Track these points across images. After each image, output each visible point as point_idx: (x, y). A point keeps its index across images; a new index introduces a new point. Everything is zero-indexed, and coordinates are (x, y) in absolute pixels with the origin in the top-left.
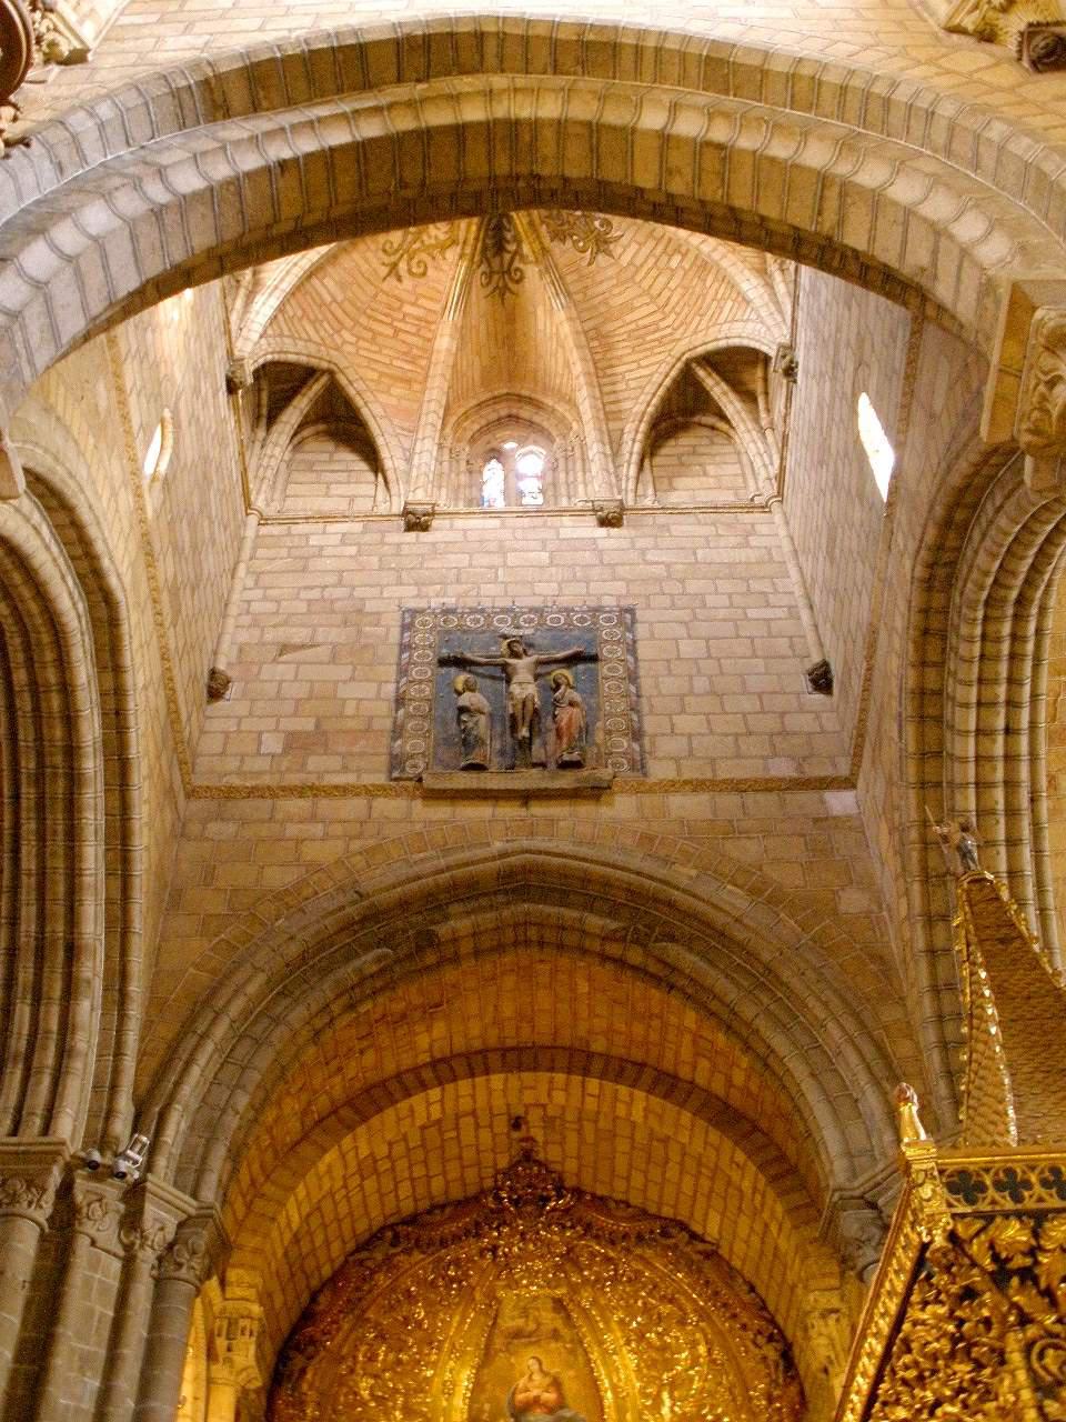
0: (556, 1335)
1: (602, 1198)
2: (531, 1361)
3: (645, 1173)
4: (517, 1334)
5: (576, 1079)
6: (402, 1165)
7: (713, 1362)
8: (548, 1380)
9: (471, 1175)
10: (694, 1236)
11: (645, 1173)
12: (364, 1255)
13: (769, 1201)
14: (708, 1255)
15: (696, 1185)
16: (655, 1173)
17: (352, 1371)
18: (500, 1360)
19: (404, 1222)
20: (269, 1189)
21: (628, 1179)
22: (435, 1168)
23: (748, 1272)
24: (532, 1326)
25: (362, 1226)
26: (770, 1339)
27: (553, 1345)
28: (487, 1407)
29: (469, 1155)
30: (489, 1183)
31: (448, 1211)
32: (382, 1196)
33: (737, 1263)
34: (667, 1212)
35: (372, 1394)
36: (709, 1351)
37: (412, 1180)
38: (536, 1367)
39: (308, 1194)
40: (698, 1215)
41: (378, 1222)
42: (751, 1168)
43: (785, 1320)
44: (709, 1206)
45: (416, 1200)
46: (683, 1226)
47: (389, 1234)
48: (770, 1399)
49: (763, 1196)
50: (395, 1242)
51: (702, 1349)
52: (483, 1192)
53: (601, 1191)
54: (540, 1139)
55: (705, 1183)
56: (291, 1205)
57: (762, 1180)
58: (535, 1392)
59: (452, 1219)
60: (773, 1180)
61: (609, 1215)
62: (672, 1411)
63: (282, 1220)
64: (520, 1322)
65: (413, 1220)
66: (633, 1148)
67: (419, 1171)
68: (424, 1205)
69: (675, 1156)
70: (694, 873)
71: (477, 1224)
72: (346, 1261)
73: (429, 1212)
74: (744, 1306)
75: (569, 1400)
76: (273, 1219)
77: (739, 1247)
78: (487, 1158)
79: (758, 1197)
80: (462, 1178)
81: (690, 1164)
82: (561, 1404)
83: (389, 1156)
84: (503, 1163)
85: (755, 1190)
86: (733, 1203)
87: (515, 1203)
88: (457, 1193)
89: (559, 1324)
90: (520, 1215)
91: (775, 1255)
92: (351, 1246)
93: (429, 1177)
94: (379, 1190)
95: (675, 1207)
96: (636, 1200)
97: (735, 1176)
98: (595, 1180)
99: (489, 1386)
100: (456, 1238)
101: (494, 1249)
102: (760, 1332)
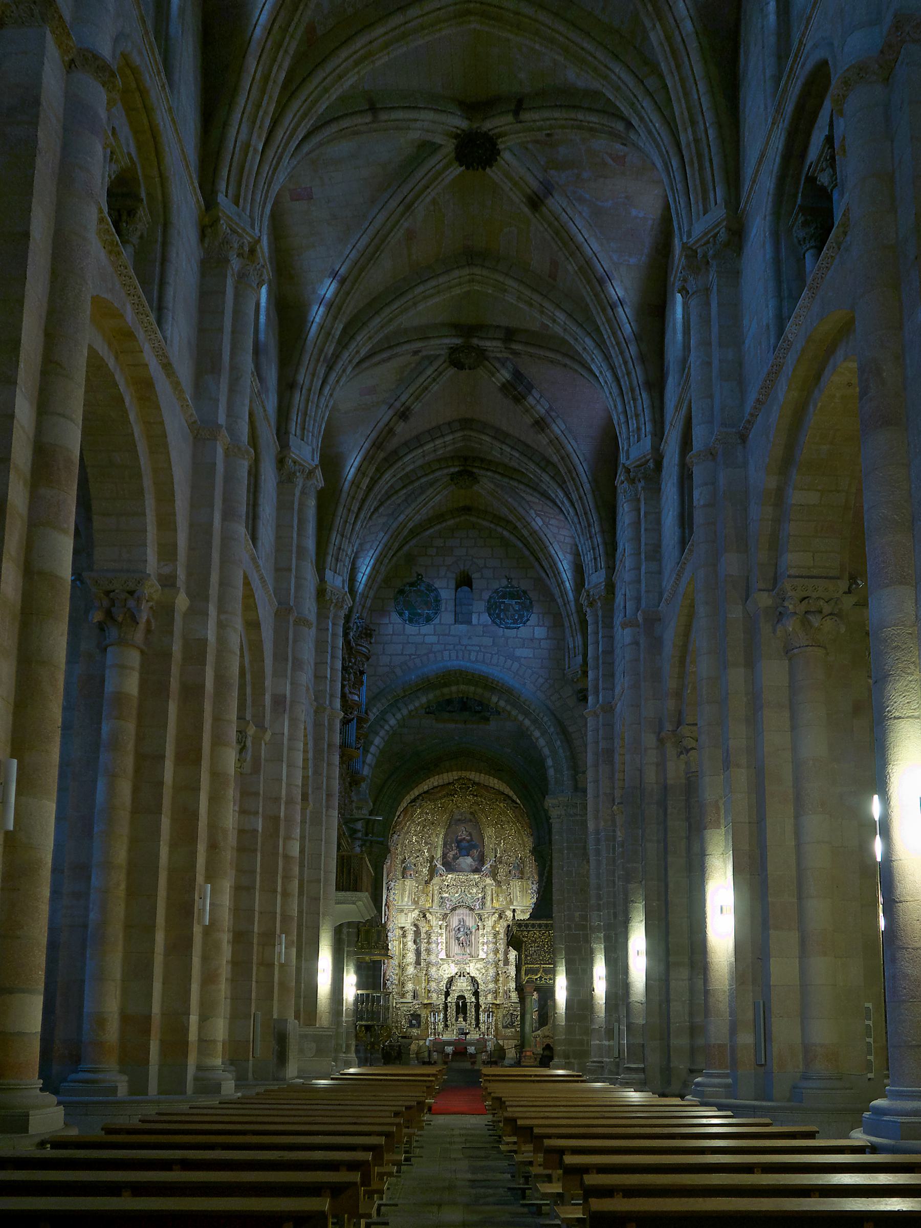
0: (471, 821)
4: (459, 820)
5: (478, 774)
8: (468, 833)
12: (413, 804)
14: (517, 807)
24: (464, 818)
27: (469, 824)
35: (416, 841)
47: (421, 798)
59: (439, 792)
61: (488, 792)
64: (460, 817)
70: (510, 751)
82: (472, 840)
89: (472, 818)
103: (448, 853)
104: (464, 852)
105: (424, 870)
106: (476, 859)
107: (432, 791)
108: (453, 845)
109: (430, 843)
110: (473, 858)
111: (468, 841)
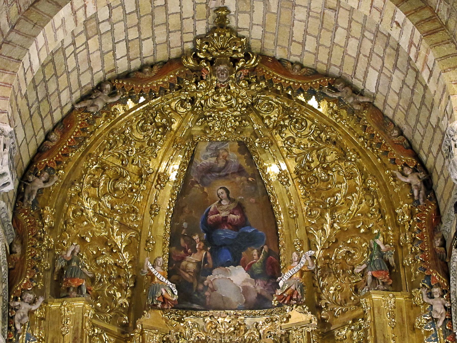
1: (280, 61)
2: (220, 191)
3: (318, 38)
4: (210, 170)
6: (119, 28)
7: (367, 189)
8: (233, 206)
9: (175, 39)
10: (356, 92)
11: (318, 38)
13: (423, 52)
15: (360, 46)
16: (326, 40)
17: (79, 194)
18: (196, 190)
19: (119, 77)
20: (14, 37)
21: (303, 44)
22: (146, 33)
23: (399, 119)
24: (222, 164)
25: (86, 80)
26: (415, 170)
27: (238, 179)
28: (185, 225)
29: (174, 21)
30: (190, 46)
31: (155, 69)
32: (103, 54)
33: (389, 113)
34: (335, 71)
35: (95, 214)
36: (364, 182)
37: (127, 41)
38: (225, 195)
39: (46, 43)
40: (360, 75)
41: (99, 76)
42: (410, 25)
43: (427, 156)
44: (369, 64)
45: (130, 60)
46: (348, 84)
47: (108, 86)
48: (412, 215)
49: (418, 48)
50: (113, 94)
51: (358, 180)
52: (184, 55)
53: (280, 54)
54: (233, 9)
55: (367, 45)
56: (33, 49)
57: (417, 34)
58: (223, 214)
60: (427, 34)
61: (287, 73)
62: (332, 226)
63: (25, 60)
64: (213, 160)
65: (127, 75)
66: (309, 16)
67: (133, 34)
68: (135, 64)
69: (343, 22)
71: (180, 80)
72: (73, 109)
73: (141, 70)
74: (395, 145)
75: (250, 219)
76: (19, 60)
77: (393, 99)
78: (188, 25)
79: (413, 49)
80: (167, 42)
81: (356, 29)
82: (244, 222)
83: (109, 19)
84: (202, 29)
85: (411, 43)
86: (389, 64)
87: (211, 63)
88: (162, 55)
89: (243, 162)
90: (214, 72)
91: (423, 103)
92: (77, 95)
93: (140, 40)
94: (100, 49)
95: (341, 67)
96: (308, 61)
97: (395, 33)
98: (276, 43)
99: (186, 209)
100: (163, 91)
101: (193, 101)
102: (405, 165)
103: (183, 259)
104: (226, 255)
105: (119, 295)
106: (259, 271)
107: (140, 75)
108: (196, 237)
109: (134, 229)
110: (249, 270)
111: (236, 227)
